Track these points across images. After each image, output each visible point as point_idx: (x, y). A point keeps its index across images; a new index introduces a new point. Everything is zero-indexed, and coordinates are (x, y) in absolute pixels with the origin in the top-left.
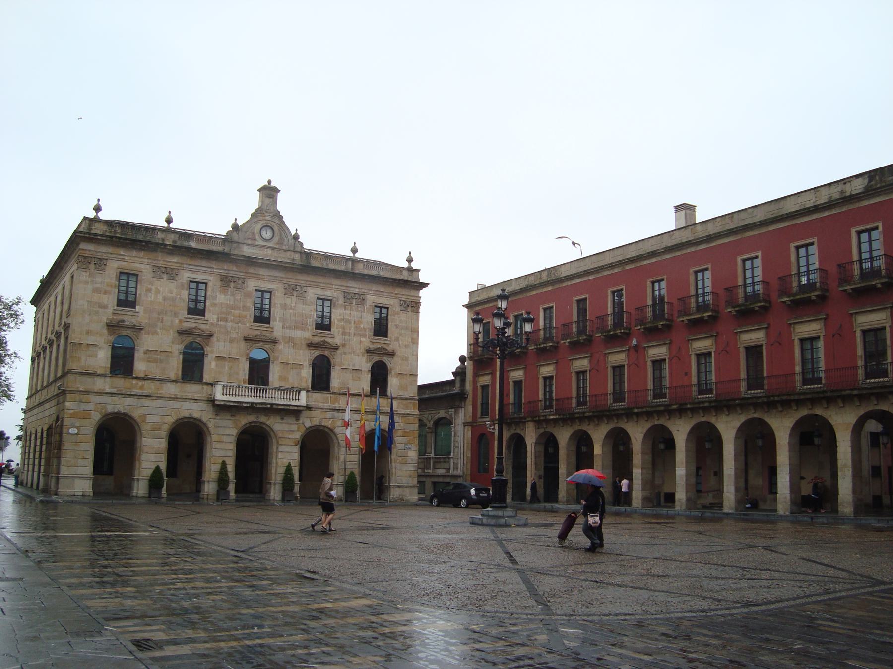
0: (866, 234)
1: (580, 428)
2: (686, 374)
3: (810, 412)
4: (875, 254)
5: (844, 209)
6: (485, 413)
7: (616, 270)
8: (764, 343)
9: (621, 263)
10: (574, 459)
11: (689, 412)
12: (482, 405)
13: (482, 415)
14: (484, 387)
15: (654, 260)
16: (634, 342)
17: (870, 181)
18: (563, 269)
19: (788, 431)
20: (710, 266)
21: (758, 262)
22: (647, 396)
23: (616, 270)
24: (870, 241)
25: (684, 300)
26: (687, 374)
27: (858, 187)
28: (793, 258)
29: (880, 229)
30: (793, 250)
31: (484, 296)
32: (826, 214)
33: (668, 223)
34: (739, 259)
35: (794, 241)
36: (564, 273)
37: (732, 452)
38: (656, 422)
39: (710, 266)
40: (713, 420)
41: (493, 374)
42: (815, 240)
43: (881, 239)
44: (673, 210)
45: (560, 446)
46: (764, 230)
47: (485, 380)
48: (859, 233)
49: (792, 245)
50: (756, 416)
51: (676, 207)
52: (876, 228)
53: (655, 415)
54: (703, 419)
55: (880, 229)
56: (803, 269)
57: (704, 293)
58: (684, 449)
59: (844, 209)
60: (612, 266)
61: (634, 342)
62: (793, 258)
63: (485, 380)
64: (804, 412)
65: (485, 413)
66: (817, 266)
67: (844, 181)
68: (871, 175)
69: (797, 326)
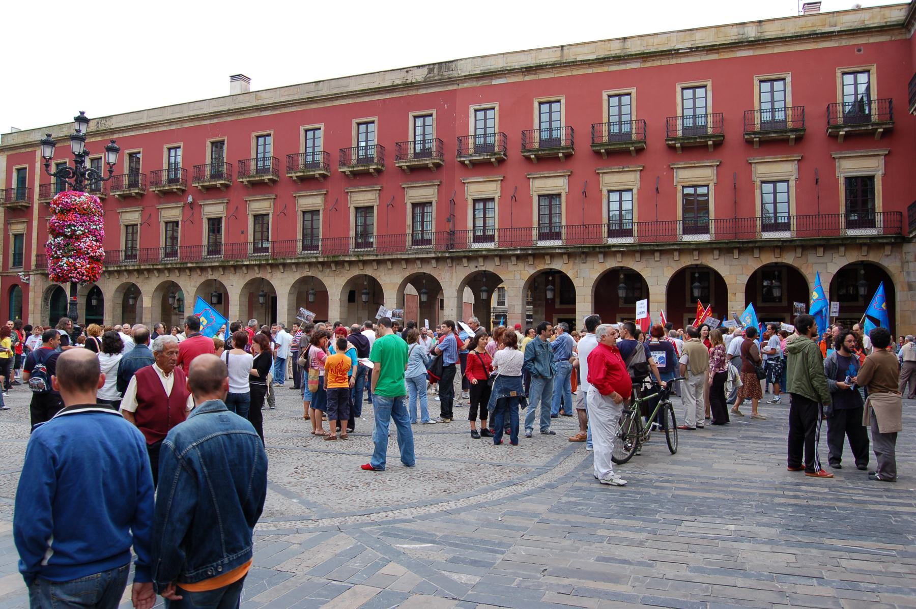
0: (422, 119)
1: (128, 280)
2: (242, 233)
3: (361, 272)
4: (427, 137)
5: (405, 94)
6: (18, 262)
7: (174, 127)
8: (321, 209)
9: (180, 120)
10: (119, 311)
11: (244, 268)
12: (14, 255)
13: (14, 265)
14: (18, 237)
15: (215, 121)
16: (190, 199)
17: (429, 73)
18: (114, 120)
19: (340, 289)
20: (272, 132)
21: (320, 134)
22: (201, 252)
23: (174, 127)
24: (424, 126)
25: (244, 163)
26: (244, 232)
27: (419, 76)
28: (354, 133)
29: (434, 116)
30: (354, 126)
31: (19, 140)
32: (388, 96)
33: (222, 88)
34: (302, 129)
35: (356, 118)
36: (114, 124)
37: (286, 307)
38: (210, 277)
39: (272, 132)
40: (268, 277)
41: (29, 224)
42: (376, 119)
43: (435, 125)
44: (229, 79)
45: (105, 298)
46: (328, 104)
47: (19, 228)
48: (415, 117)
49: (355, 121)
50: (310, 274)
51: (232, 77)
52: (431, 115)
53: (209, 270)
54: (258, 276)
55: (434, 116)
56: (363, 144)
57: (264, 157)
58: (237, 303)
59: (405, 94)
60: (170, 122)
61: (190, 199)
62: (354, 133)
63: (19, 228)
64: (356, 272)
65: (18, 262)
66: (376, 142)
67: (407, 70)
68: (431, 67)
69: (354, 195)
